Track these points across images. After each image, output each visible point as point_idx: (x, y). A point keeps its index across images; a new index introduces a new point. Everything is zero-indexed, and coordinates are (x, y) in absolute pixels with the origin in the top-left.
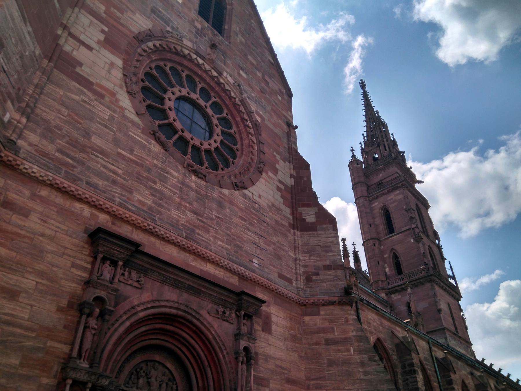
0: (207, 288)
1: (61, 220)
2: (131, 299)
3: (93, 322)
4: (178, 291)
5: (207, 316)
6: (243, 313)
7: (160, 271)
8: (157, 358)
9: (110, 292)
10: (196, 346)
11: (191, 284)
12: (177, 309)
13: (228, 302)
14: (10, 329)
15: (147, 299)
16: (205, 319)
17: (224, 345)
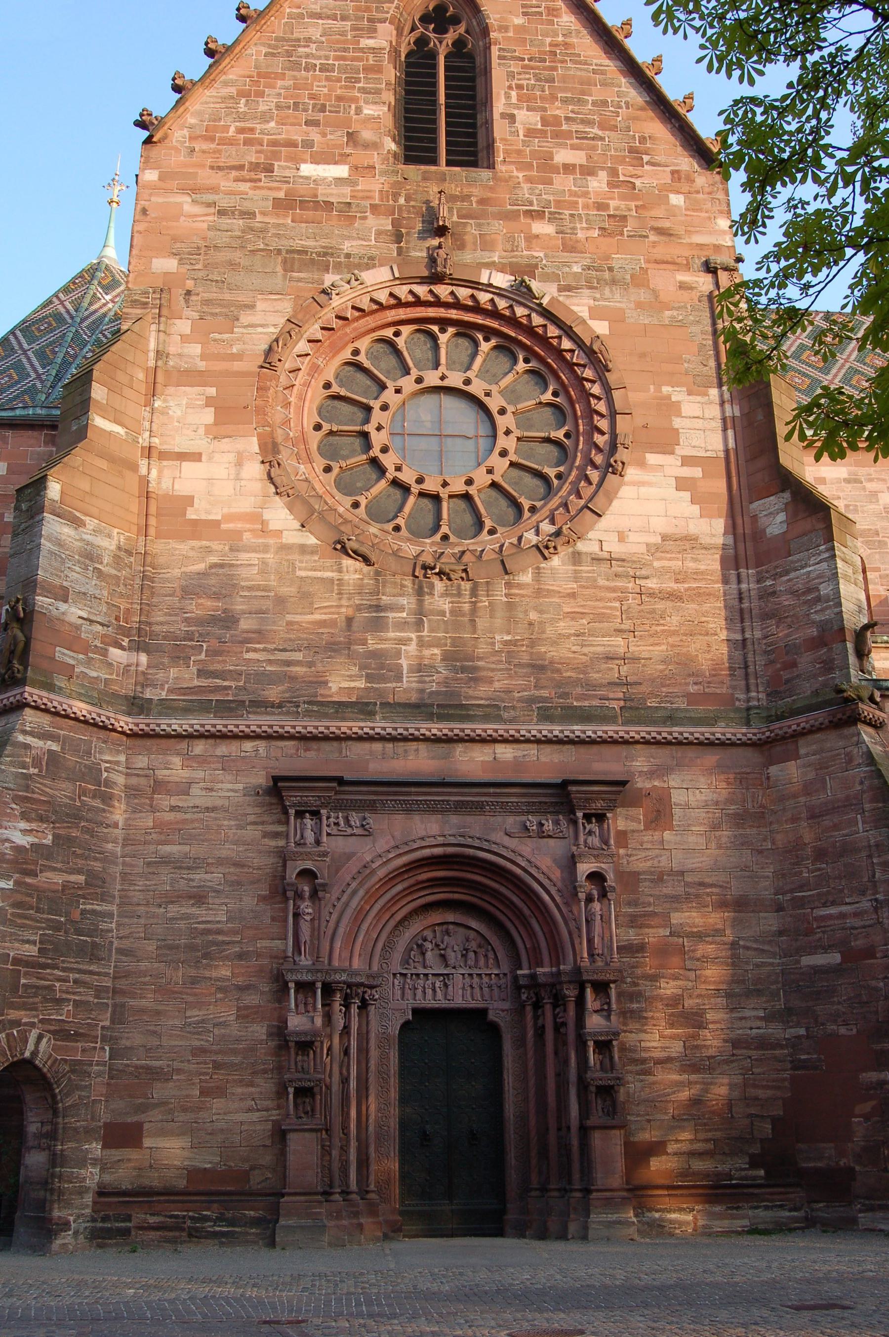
1: (229, 778)
3: (306, 907)
5: (506, 841)
6: (580, 814)
12: (444, 845)
14: (210, 938)
15: (387, 847)
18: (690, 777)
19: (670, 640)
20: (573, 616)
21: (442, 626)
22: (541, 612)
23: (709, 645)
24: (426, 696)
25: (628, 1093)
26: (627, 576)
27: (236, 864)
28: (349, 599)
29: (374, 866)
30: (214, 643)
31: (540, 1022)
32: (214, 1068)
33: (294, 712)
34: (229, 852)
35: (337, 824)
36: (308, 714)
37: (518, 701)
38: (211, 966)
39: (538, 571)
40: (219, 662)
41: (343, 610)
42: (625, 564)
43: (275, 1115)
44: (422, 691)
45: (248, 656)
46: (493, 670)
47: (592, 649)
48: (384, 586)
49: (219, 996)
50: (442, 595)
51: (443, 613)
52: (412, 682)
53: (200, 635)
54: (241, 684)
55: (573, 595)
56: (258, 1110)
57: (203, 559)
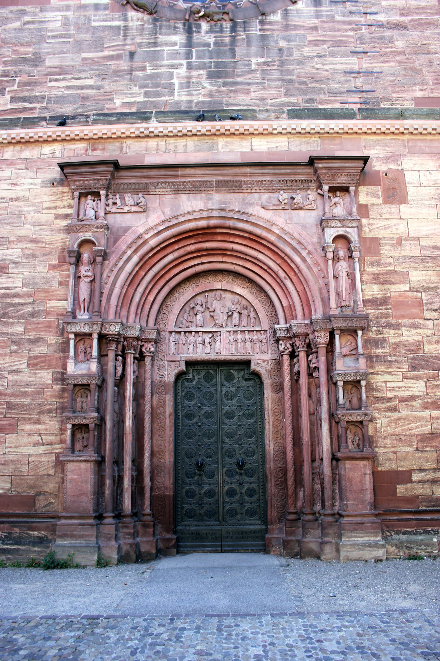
0: (251, 175)
2: (134, 228)
4: (204, 195)
5: (263, 213)
6: (326, 188)
7: (164, 180)
8: (218, 285)
9: (96, 230)
10: (260, 256)
11: (221, 178)
13: (296, 181)
14: (9, 300)
15: (157, 221)
16: (259, 218)
17: (300, 243)
18: (420, 162)
19: (398, 58)
20: (316, 43)
21: (207, 54)
22: (289, 41)
23: (430, 61)
24: (194, 105)
25: (376, 428)
26: (360, 13)
27: (32, 241)
28: (132, 39)
29: (147, 237)
30: (25, 78)
31: (296, 369)
32: (8, 408)
33: (84, 122)
34: (27, 232)
35: (115, 204)
36: (95, 122)
37: (271, 106)
38: (8, 323)
39: (286, 13)
40: (27, 91)
41: (127, 47)
42: (358, 4)
43: (58, 448)
44: (190, 102)
45: (50, 84)
46: (249, 84)
47: (332, 66)
48: (160, 29)
49: (14, 348)
50: (207, 32)
51: (208, 45)
52: (182, 95)
53: (15, 72)
54: (44, 105)
55: (315, 28)
56: (43, 444)
57: (19, 19)
